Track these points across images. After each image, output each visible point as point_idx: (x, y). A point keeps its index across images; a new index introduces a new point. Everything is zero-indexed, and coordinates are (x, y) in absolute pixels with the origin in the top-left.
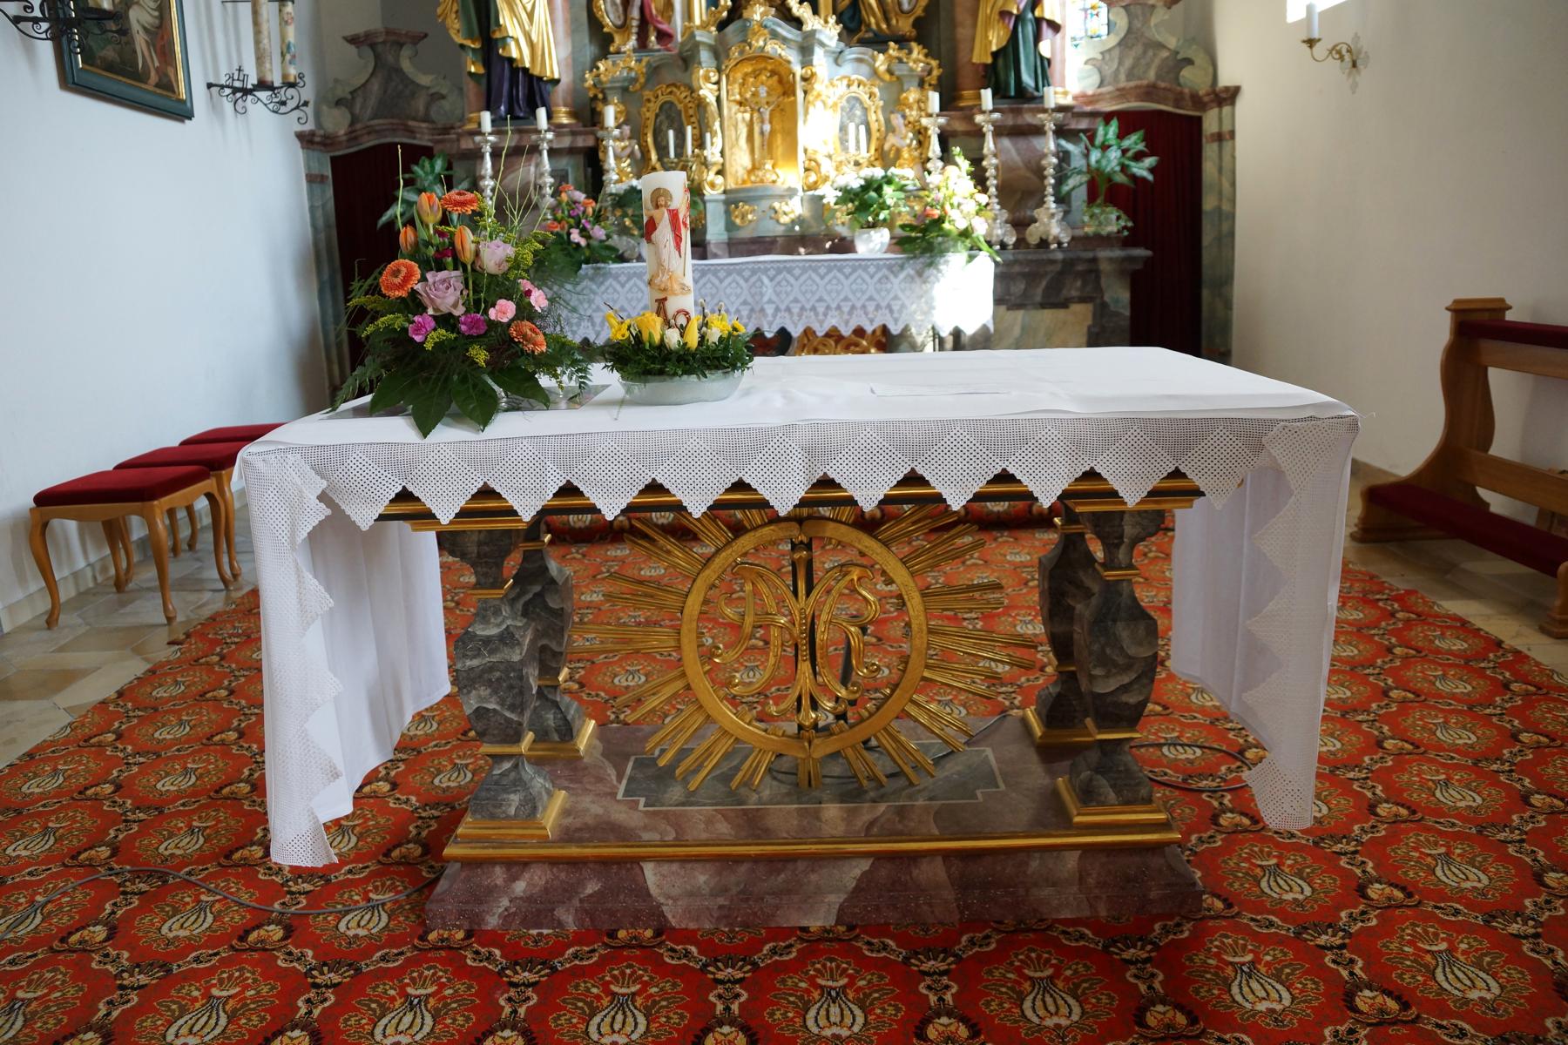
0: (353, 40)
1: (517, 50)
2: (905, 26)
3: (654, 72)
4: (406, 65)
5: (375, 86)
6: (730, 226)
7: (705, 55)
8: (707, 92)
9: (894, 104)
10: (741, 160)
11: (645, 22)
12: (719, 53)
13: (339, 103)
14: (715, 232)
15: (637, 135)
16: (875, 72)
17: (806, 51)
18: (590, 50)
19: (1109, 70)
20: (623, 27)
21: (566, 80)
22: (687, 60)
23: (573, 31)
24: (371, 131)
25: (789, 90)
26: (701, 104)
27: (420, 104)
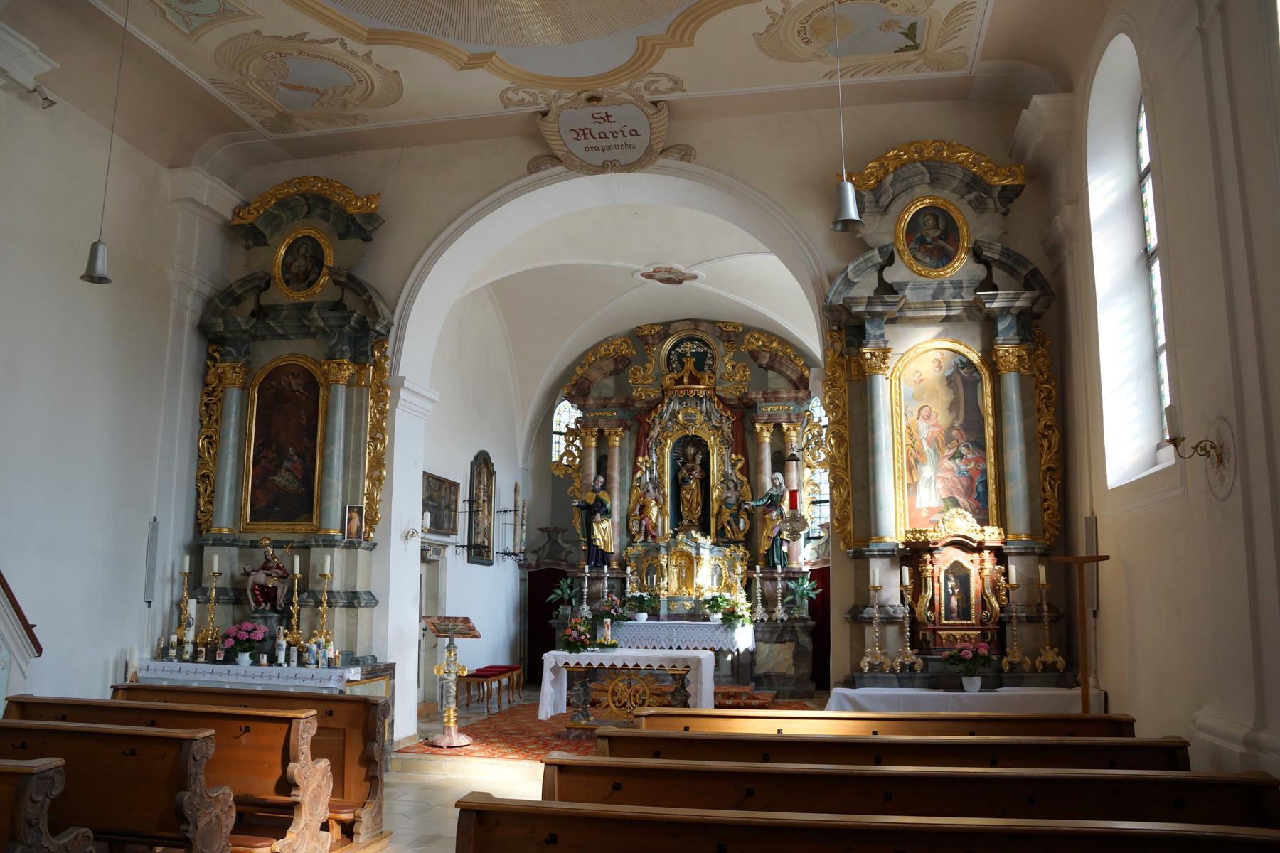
0: (541, 530)
1: (600, 543)
2: (741, 537)
3: (647, 552)
4: (559, 540)
5: (548, 547)
6: (669, 610)
7: (663, 550)
8: (663, 562)
9: (732, 568)
10: (674, 586)
11: (647, 532)
12: (668, 548)
13: (534, 552)
14: (663, 612)
15: (640, 575)
16: (725, 555)
17: (698, 548)
18: (626, 540)
19: (821, 552)
20: (639, 532)
21: (617, 552)
22: (658, 550)
23: (621, 533)
24: (544, 563)
25: (692, 563)
26: (661, 566)
27: (563, 555)
